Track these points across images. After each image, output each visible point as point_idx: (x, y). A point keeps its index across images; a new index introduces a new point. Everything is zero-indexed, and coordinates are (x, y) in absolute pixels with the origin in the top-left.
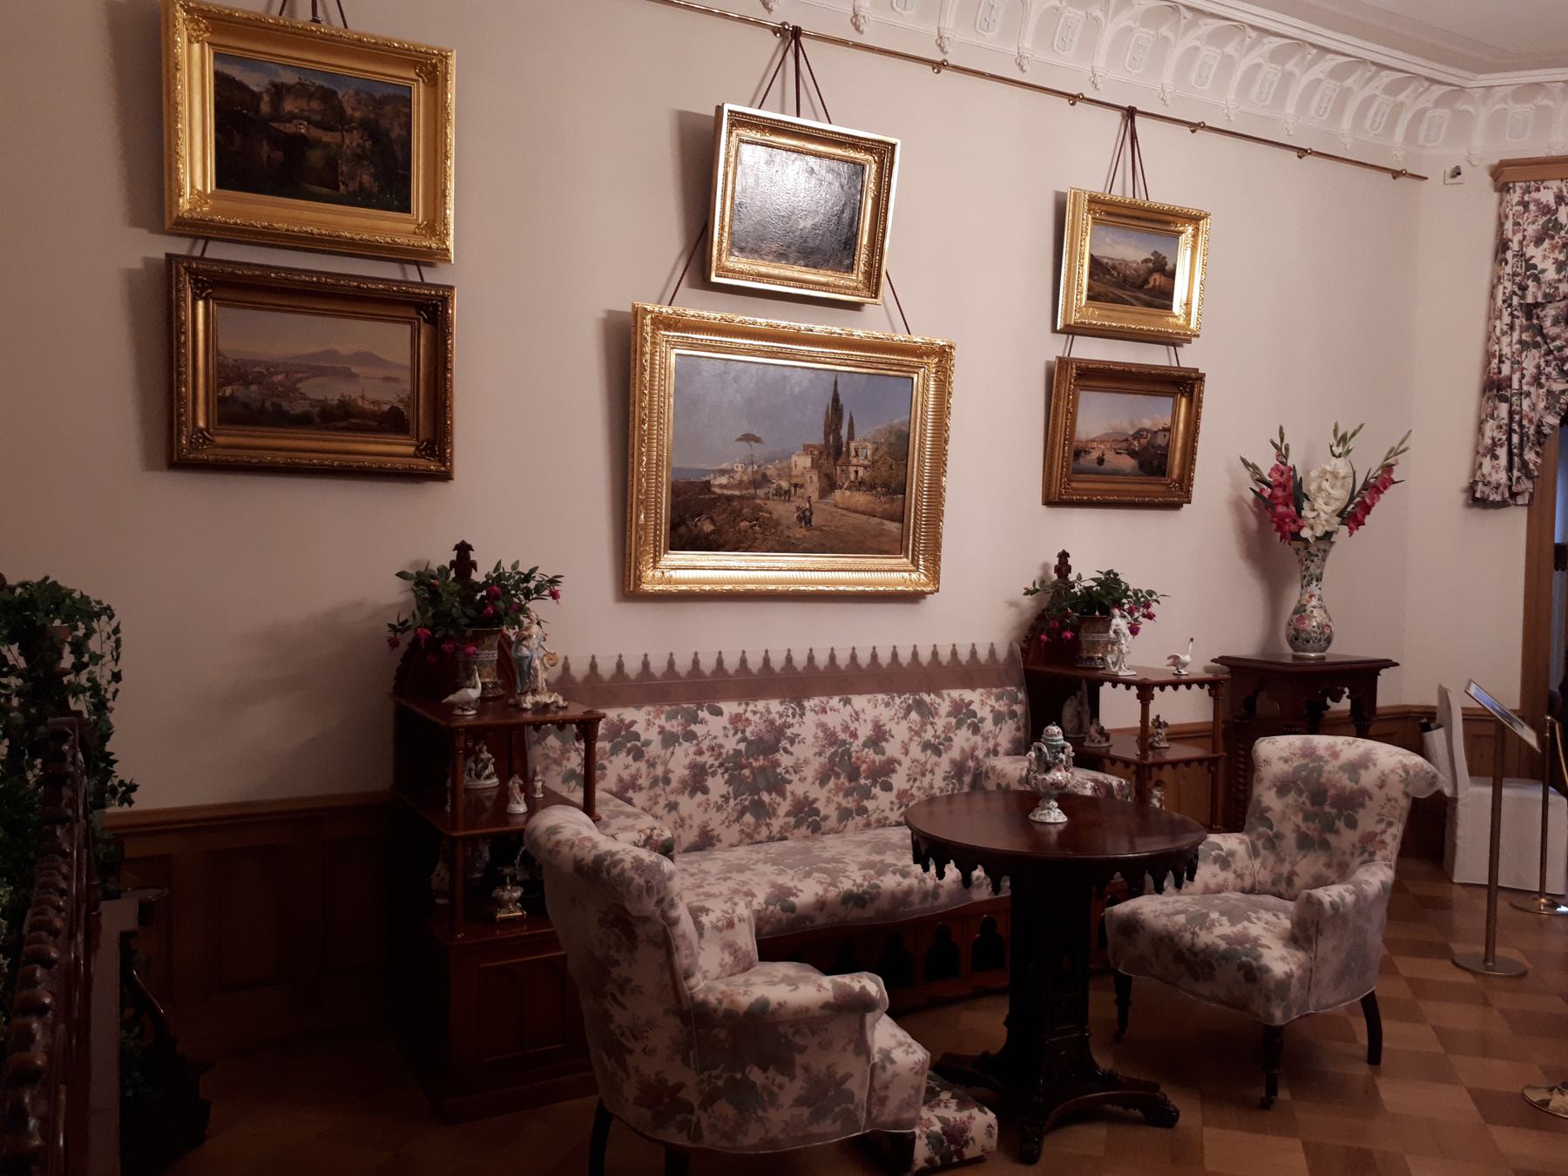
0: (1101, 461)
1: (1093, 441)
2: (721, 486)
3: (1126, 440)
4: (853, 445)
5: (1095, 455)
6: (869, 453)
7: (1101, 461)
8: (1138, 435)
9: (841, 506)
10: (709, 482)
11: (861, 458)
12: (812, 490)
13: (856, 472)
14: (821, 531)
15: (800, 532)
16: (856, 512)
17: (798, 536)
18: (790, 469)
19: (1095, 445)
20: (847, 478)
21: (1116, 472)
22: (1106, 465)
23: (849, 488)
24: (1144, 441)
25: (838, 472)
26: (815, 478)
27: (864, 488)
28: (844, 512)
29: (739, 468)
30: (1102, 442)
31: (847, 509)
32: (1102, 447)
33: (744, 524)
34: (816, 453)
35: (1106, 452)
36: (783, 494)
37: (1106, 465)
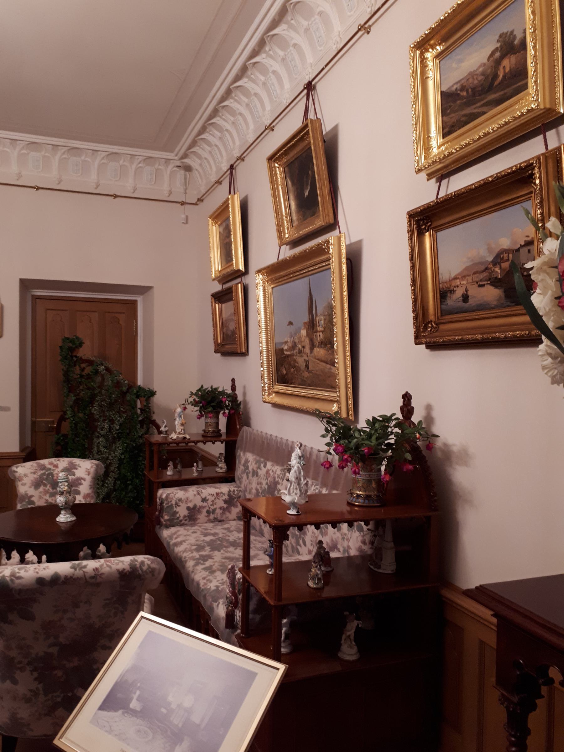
0: (465, 298)
1: (455, 278)
2: (286, 350)
3: (486, 269)
4: (317, 319)
5: (459, 292)
6: (323, 322)
7: (465, 298)
8: (498, 259)
9: (317, 358)
10: (283, 349)
11: (321, 326)
12: (307, 350)
13: (320, 335)
14: (312, 373)
15: (306, 374)
16: (322, 361)
17: (306, 376)
18: (301, 337)
19: (458, 282)
20: (317, 340)
21: (482, 307)
22: (472, 302)
23: (318, 347)
24: (506, 265)
25: (314, 337)
26: (308, 342)
27: (323, 346)
28: (318, 362)
29: (289, 340)
30: (464, 277)
31: (318, 359)
32: (464, 282)
33: (292, 370)
34: (307, 327)
35: (469, 287)
36: (300, 352)
37: (472, 302)
